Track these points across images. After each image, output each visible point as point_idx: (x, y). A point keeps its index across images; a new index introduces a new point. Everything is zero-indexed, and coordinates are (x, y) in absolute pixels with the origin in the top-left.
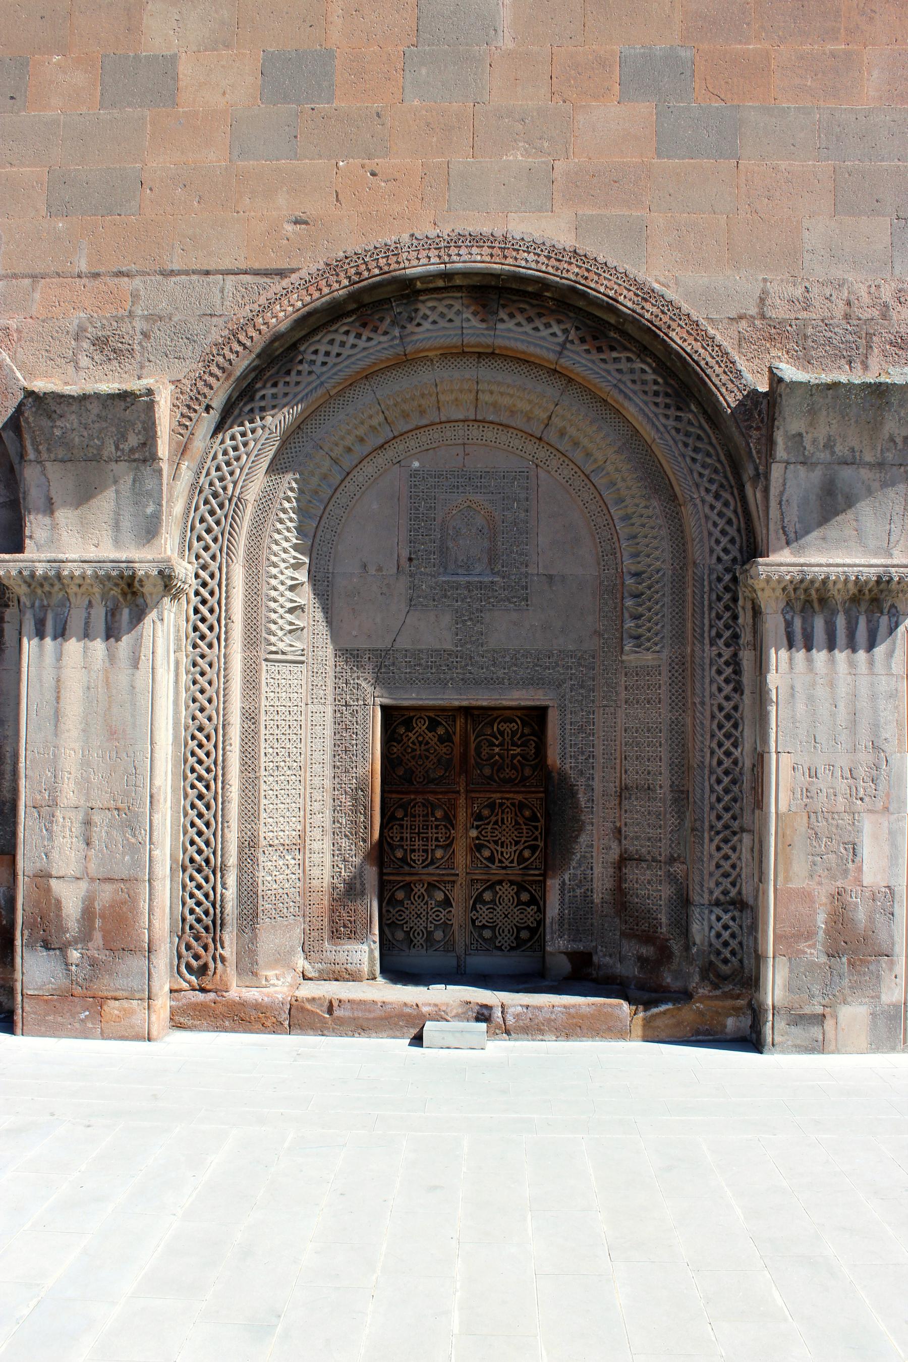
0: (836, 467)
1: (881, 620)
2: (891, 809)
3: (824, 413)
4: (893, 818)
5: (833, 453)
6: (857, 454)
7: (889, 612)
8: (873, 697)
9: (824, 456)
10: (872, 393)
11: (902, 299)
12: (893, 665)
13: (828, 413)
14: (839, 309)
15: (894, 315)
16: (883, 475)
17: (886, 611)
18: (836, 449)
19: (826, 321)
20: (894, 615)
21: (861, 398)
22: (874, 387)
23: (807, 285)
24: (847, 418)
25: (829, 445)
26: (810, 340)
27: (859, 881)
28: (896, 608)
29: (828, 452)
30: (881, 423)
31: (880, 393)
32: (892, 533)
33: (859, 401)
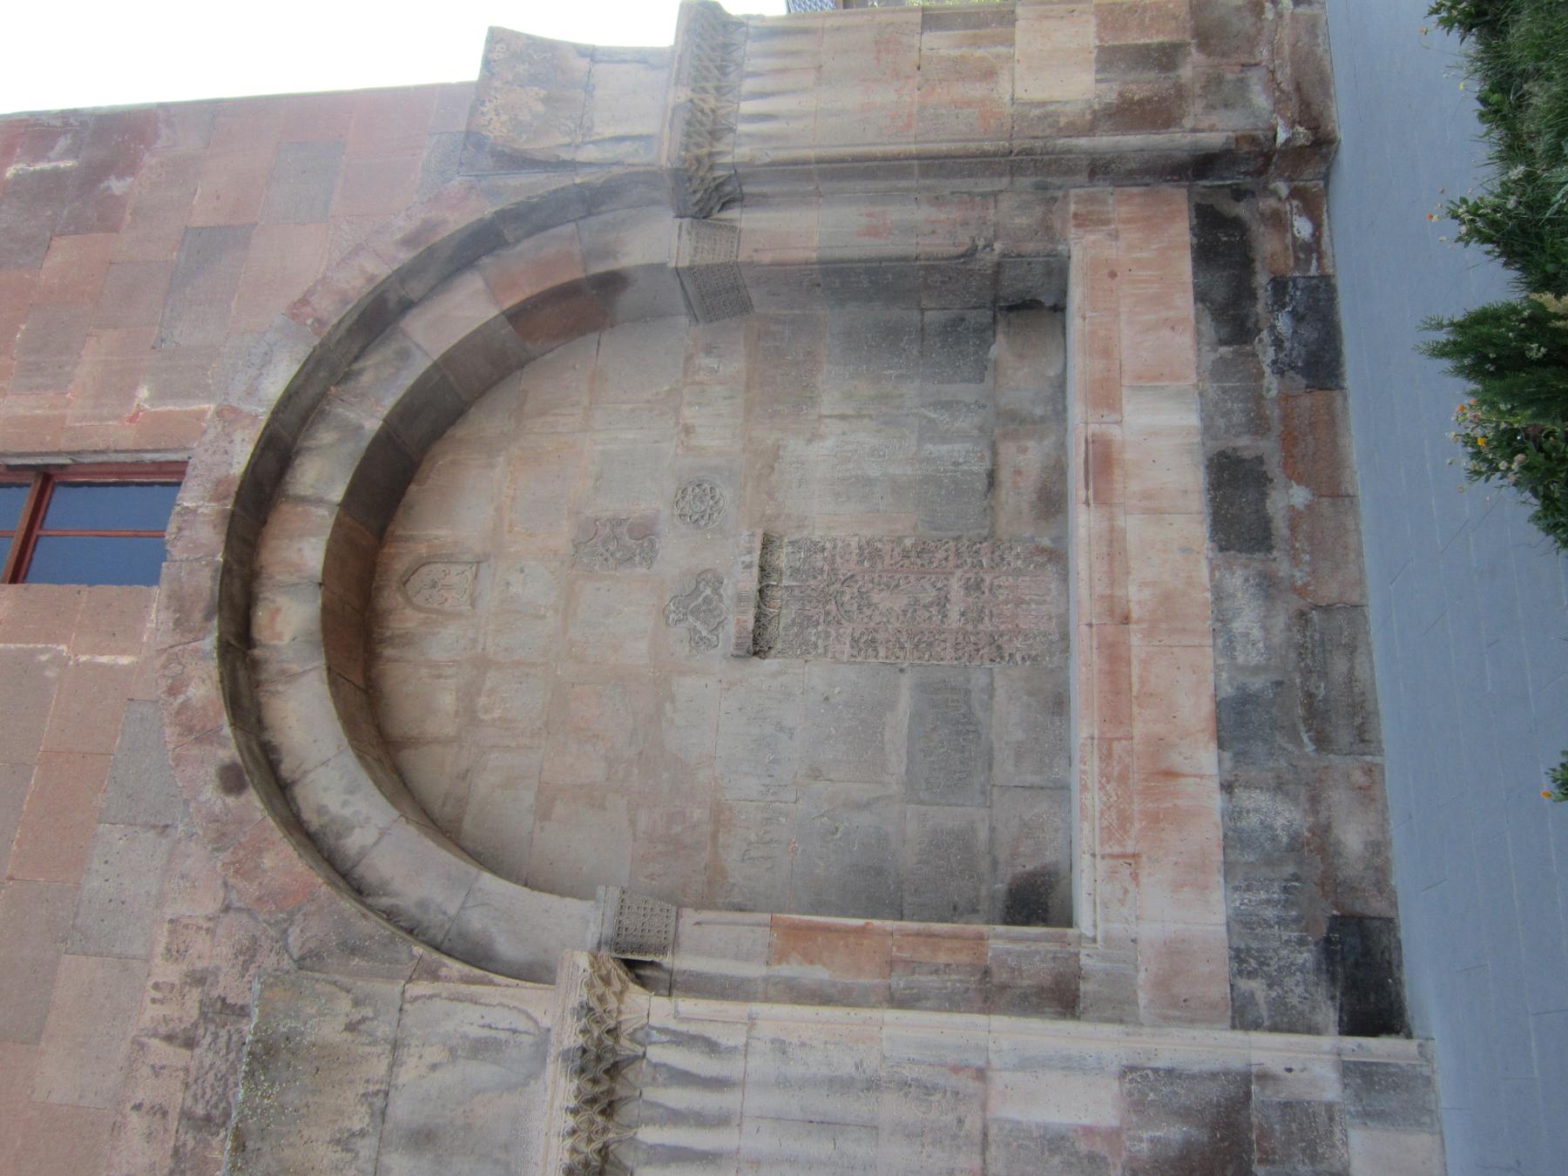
0: (389, 1126)
1: (655, 1059)
2: (980, 1063)
3: (288, 1152)
4: (996, 1061)
5: (362, 1134)
6: (372, 1088)
7: (642, 1044)
8: (783, 1083)
9: (366, 1148)
10: (265, 1068)
11: (182, 948)
12: (732, 1043)
13: (291, 1145)
14: (175, 1056)
15: (199, 965)
16: (414, 1042)
17: (640, 1050)
18: (357, 1127)
19: (191, 1080)
20: (648, 1035)
21: (271, 1086)
22: (256, 1066)
23: (129, 1106)
24: (303, 1111)
25: (344, 1142)
26: (214, 1111)
27: (1113, 1135)
28: (635, 1030)
29: (360, 1144)
30: (323, 1047)
31: (268, 1053)
32: (513, 1026)
33: (277, 1088)
